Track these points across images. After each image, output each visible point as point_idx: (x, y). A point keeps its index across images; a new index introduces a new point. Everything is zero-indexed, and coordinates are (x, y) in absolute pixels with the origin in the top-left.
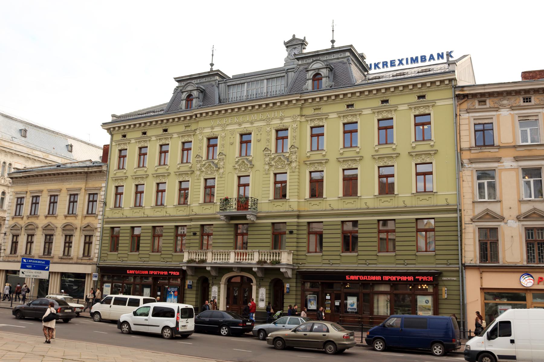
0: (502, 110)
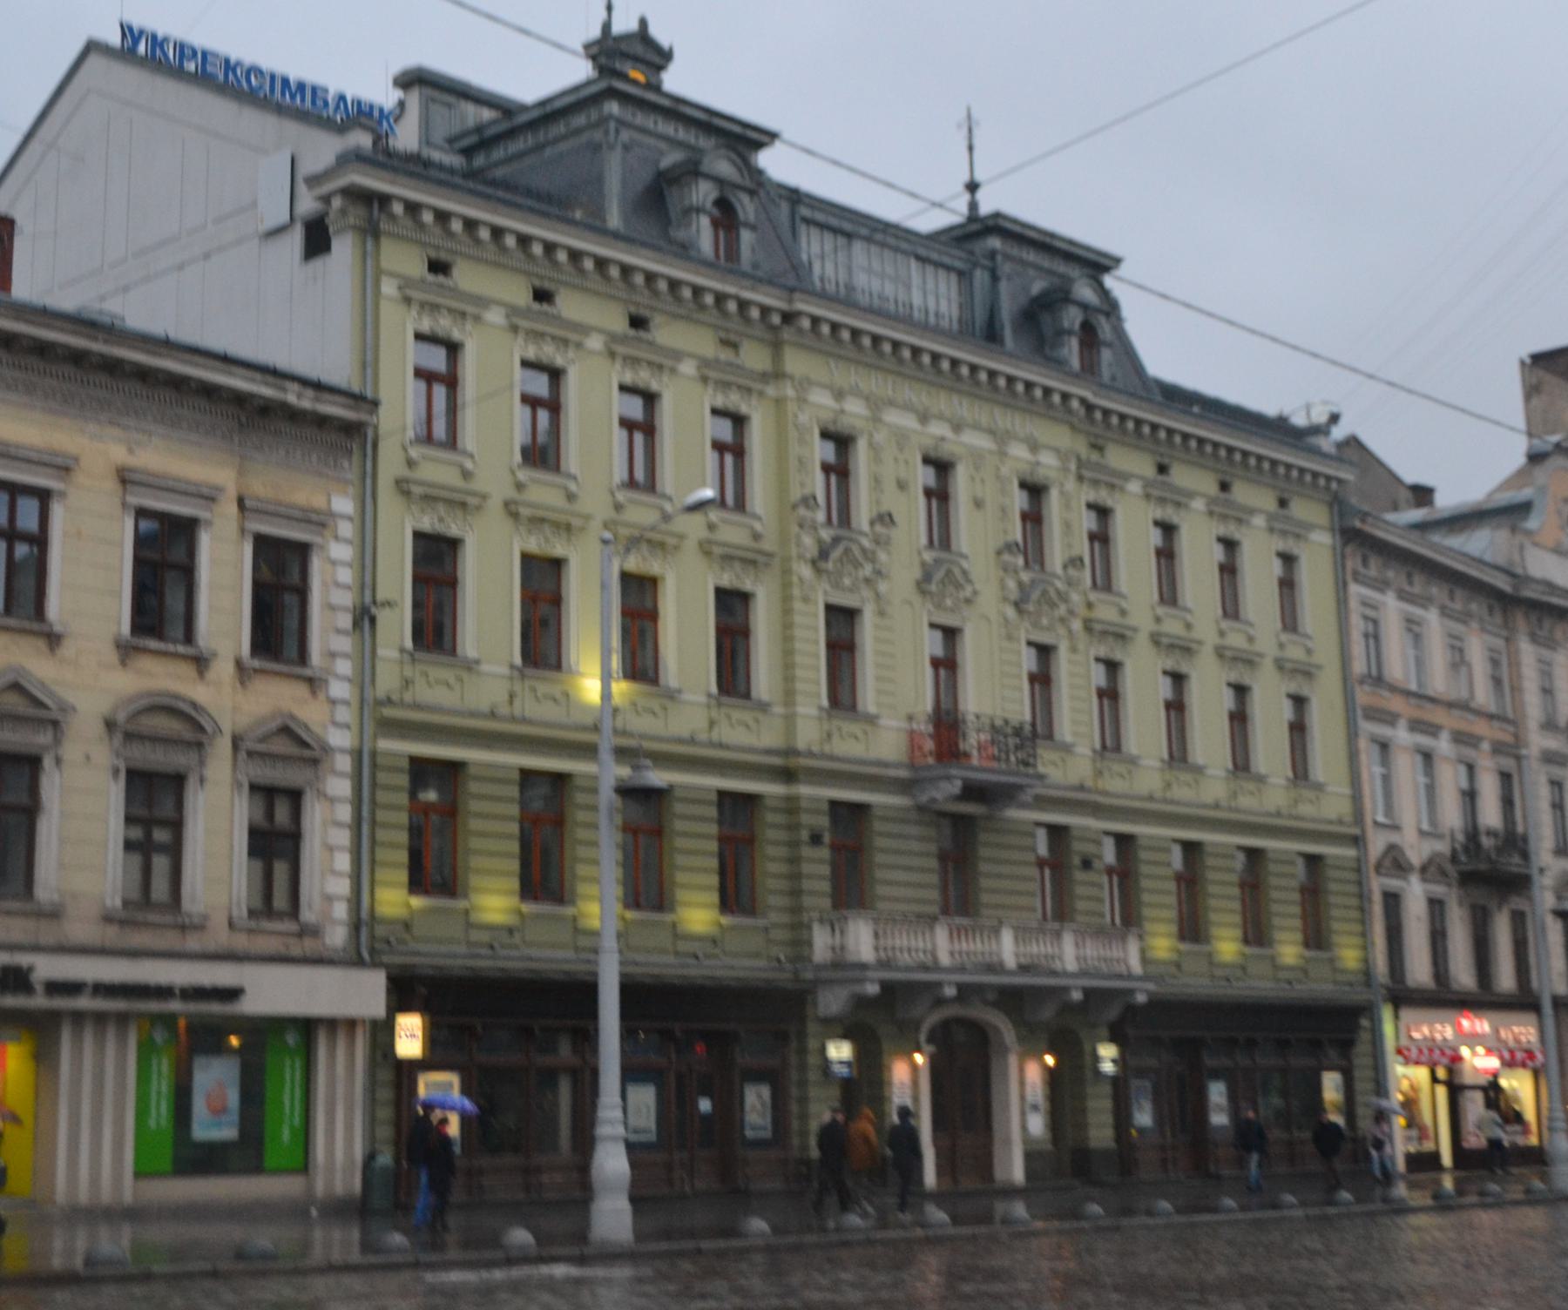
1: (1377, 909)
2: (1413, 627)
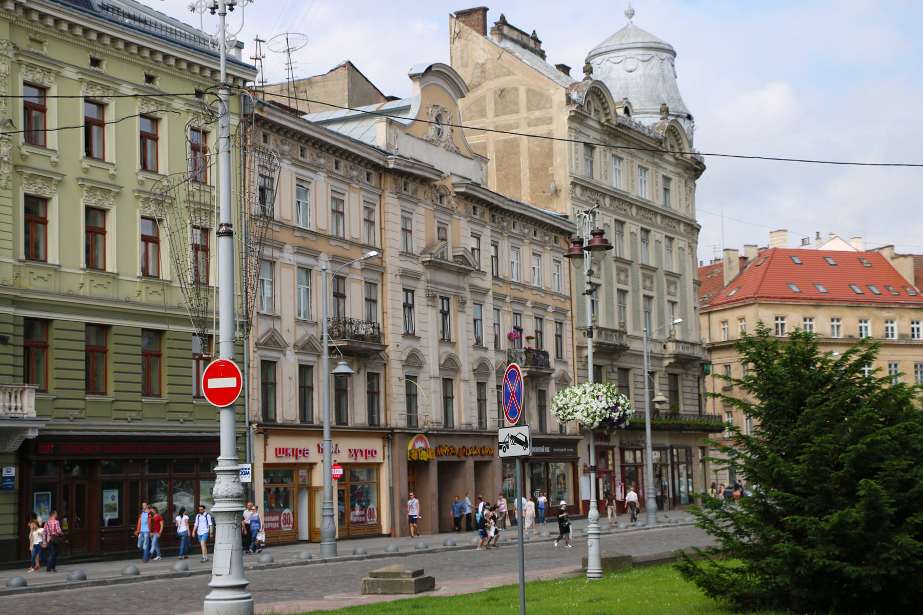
0: (285, 161)
2: (302, 186)
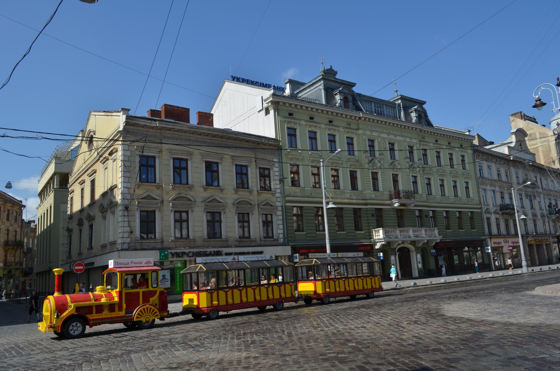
1: (485, 221)
2: (489, 167)
